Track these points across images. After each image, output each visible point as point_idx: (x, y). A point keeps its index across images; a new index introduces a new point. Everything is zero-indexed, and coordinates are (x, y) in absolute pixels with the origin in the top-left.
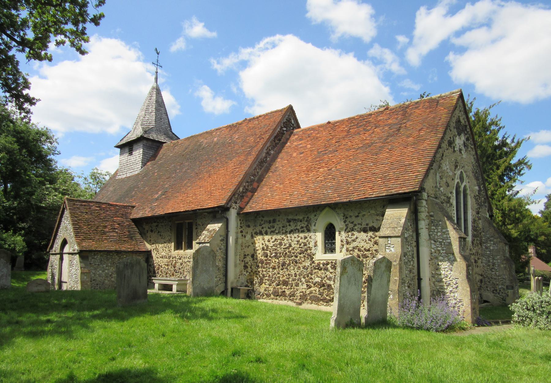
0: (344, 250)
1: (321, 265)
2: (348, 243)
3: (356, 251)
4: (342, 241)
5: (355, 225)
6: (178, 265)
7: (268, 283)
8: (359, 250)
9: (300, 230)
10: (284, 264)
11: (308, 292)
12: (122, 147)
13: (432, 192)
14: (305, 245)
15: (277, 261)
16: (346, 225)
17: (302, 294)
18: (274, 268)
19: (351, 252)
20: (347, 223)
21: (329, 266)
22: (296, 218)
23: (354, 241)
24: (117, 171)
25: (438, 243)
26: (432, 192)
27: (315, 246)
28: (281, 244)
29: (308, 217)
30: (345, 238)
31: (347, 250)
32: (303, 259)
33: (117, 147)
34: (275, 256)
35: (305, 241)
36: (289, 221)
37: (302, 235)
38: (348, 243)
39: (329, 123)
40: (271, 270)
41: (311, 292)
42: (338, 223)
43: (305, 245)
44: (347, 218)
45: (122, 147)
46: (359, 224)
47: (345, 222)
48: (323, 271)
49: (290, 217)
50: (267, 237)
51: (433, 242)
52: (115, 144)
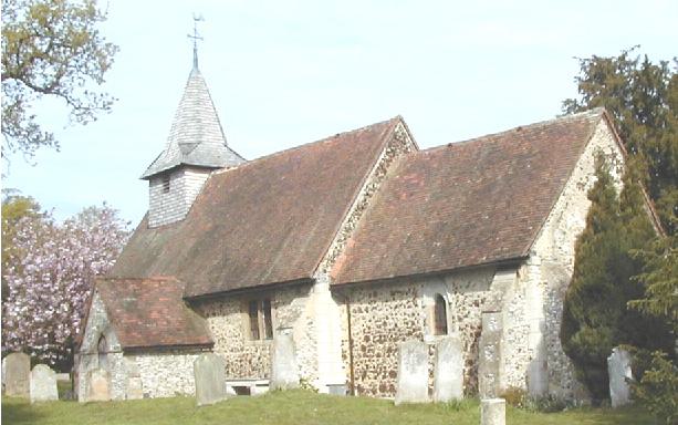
2: (460, 320)
6: (255, 360)
7: (372, 375)
10: (390, 350)
12: (152, 179)
13: (547, 254)
14: (413, 324)
15: (381, 346)
18: (378, 356)
22: (401, 289)
23: (466, 316)
24: (147, 214)
26: (547, 254)
28: (385, 323)
33: (146, 178)
34: (381, 342)
36: (393, 294)
37: (410, 311)
38: (460, 320)
39: (450, 145)
40: (375, 358)
42: (449, 297)
43: (413, 324)
45: (152, 179)
49: (394, 289)
50: (368, 316)
52: (141, 174)
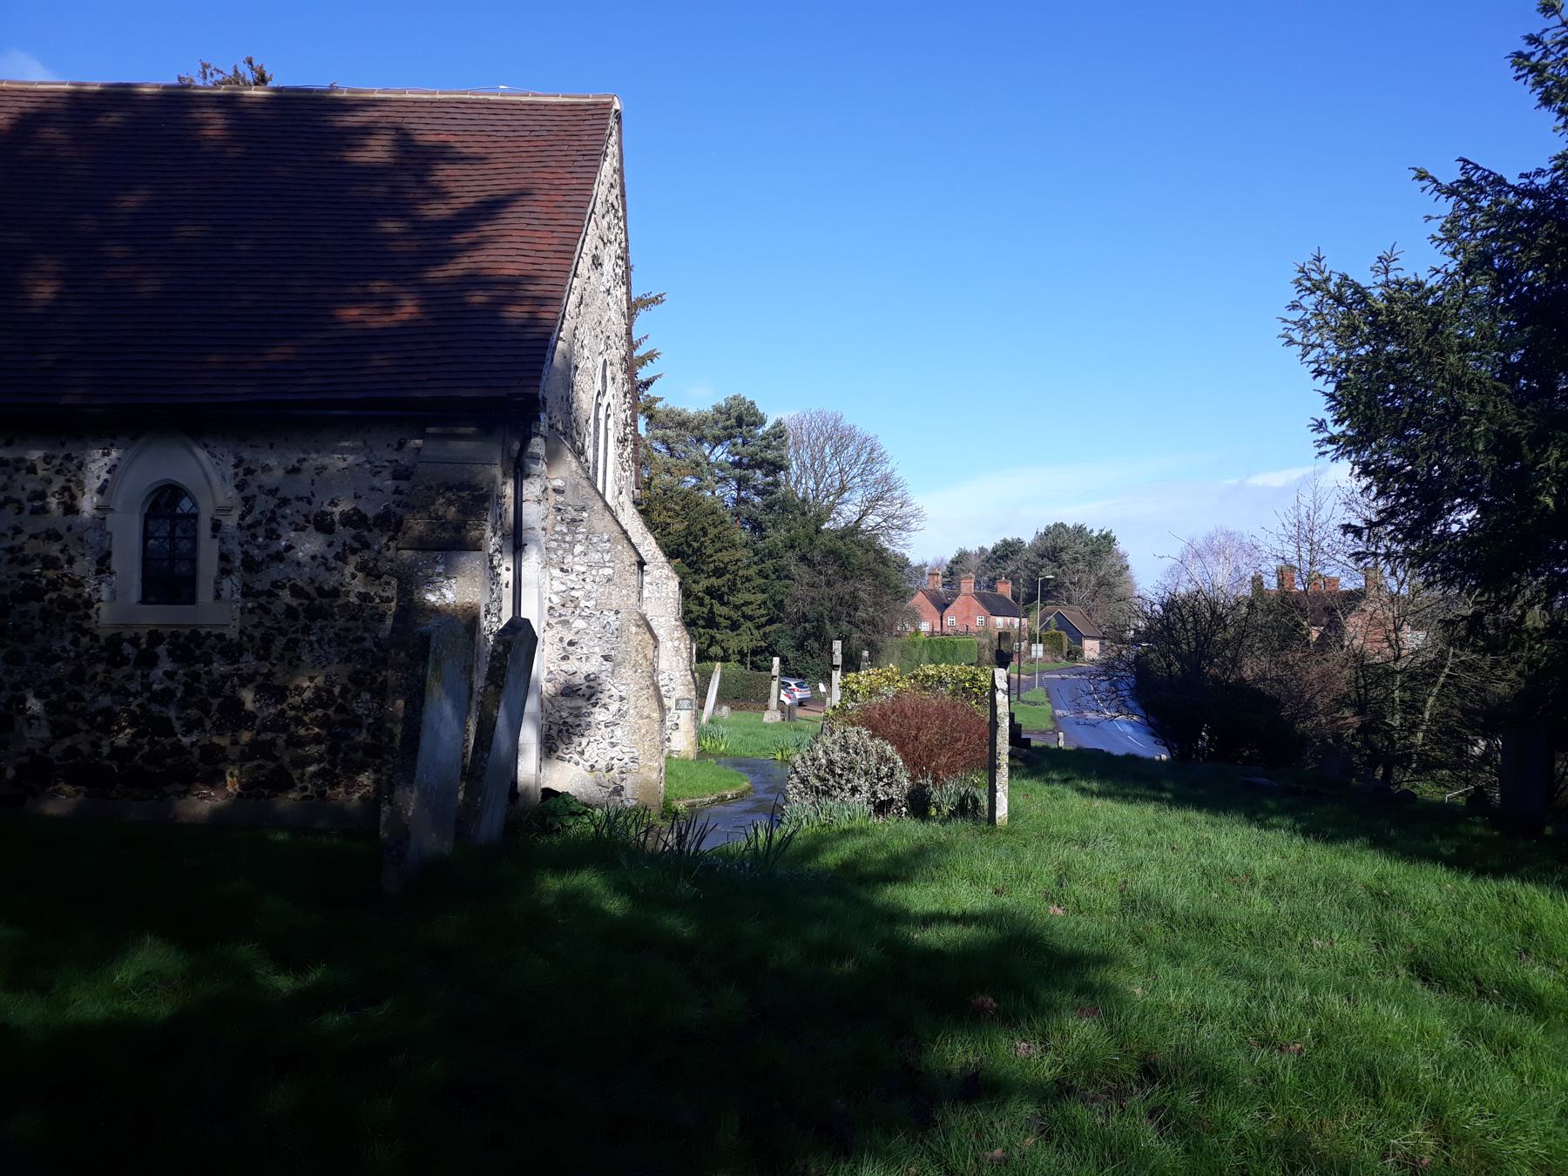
0: (230, 585)
1: (127, 649)
3: (285, 595)
4: (224, 557)
5: (284, 502)
8: (296, 591)
9: (28, 506)
11: (57, 749)
16: (246, 500)
17: (26, 760)
19: (263, 600)
20: (247, 492)
21: (161, 650)
23: (279, 557)
25: (573, 577)
27: (98, 572)
29: (68, 457)
30: (237, 550)
31: (247, 591)
32: (38, 624)
35: (54, 549)
41: (72, 752)
44: (249, 472)
46: (300, 499)
47: (240, 487)
48: (126, 669)
51: (556, 572)
